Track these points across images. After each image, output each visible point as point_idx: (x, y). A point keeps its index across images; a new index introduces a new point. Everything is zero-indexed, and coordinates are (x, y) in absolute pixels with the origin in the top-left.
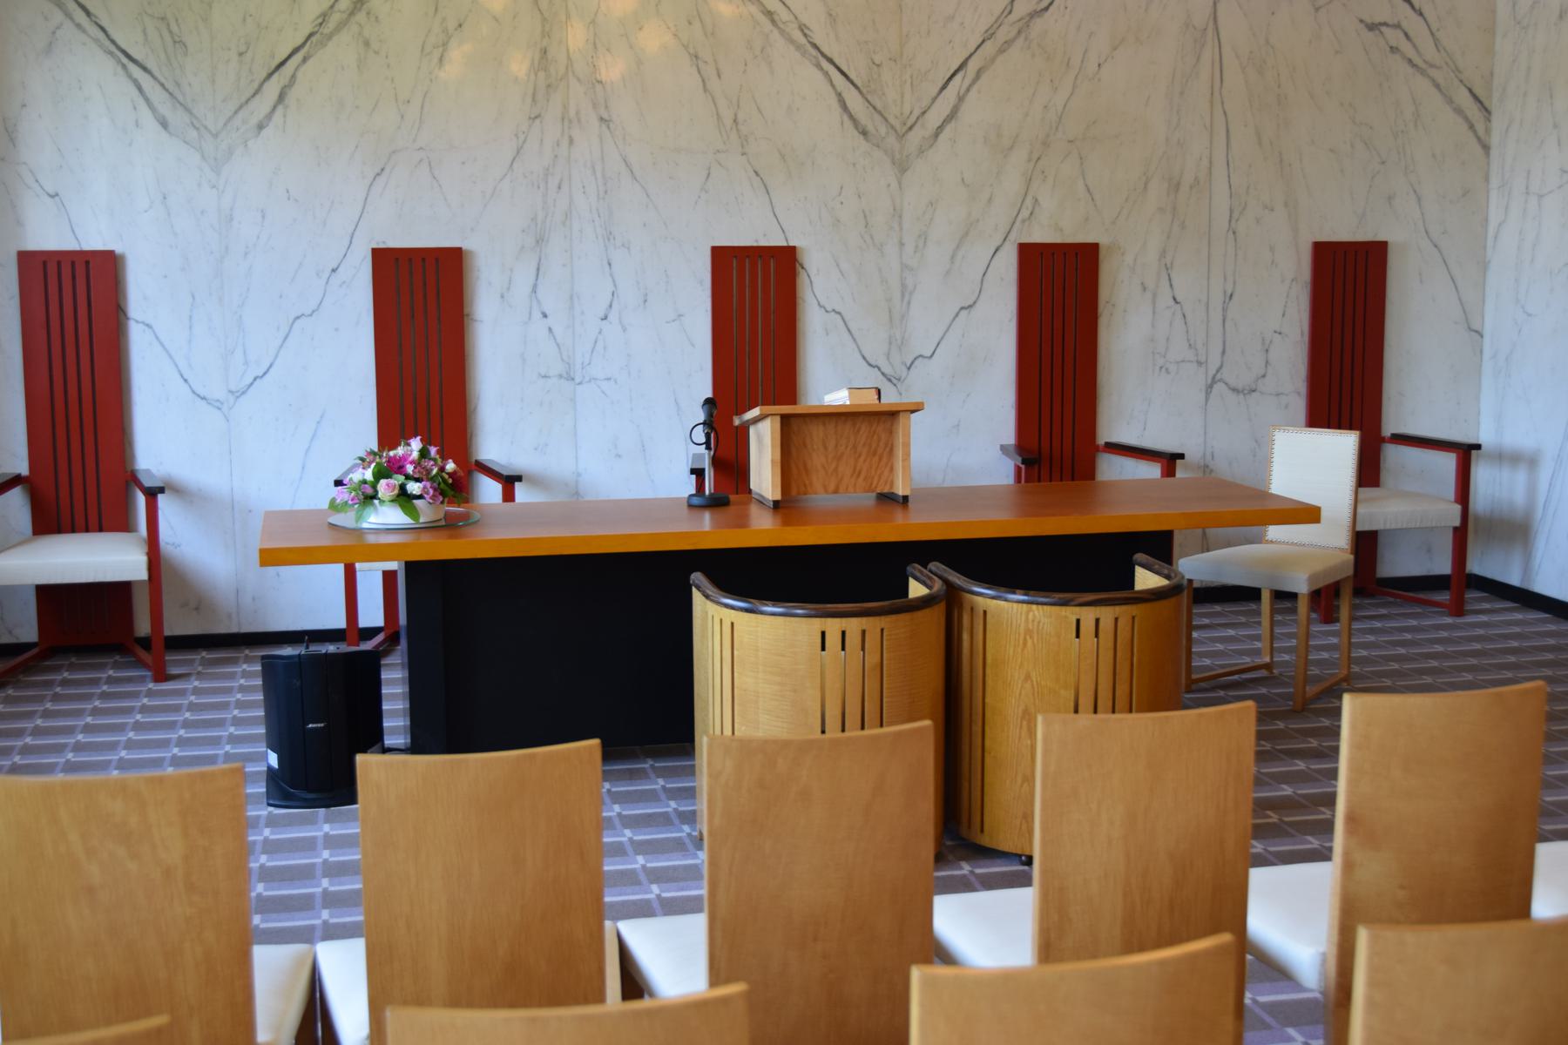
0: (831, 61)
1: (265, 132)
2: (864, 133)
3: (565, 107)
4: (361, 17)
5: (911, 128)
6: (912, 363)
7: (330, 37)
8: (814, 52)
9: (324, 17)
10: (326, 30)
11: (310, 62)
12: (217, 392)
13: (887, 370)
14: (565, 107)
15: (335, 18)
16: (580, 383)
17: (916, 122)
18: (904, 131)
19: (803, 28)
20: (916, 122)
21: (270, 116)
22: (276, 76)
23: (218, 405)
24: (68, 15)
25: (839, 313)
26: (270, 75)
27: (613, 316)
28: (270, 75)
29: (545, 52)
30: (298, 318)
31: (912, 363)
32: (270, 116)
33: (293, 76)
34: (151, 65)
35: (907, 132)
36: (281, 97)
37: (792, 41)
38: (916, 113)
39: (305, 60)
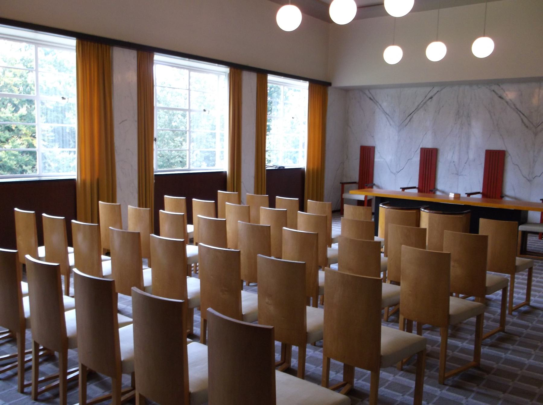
0: (520, 112)
1: (407, 126)
2: (527, 127)
3: (462, 122)
4: (425, 105)
5: (539, 126)
6: (535, 177)
7: (419, 109)
8: (516, 110)
9: (419, 105)
10: (419, 108)
11: (415, 114)
12: (395, 172)
13: (528, 178)
14: (462, 122)
15: (420, 106)
16: (460, 175)
17: (540, 125)
18: (537, 126)
19: (514, 105)
20: (540, 125)
21: (407, 124)
22: (409, 116)
23: (394, 174)
24: (378, 107)
25: (517, 165)
26: (409, 116)
27: (467, 163)
28: (409, 116)
29: (458, 111)
30: (409, 160)
31: (535, 177)
32: (407, 124)
33: (412, 117)
34: (390, 115)
35: (537, 127)
36: (410, 120)
37: (511, 108)
38: (541, 122)
39: (415, 113)
